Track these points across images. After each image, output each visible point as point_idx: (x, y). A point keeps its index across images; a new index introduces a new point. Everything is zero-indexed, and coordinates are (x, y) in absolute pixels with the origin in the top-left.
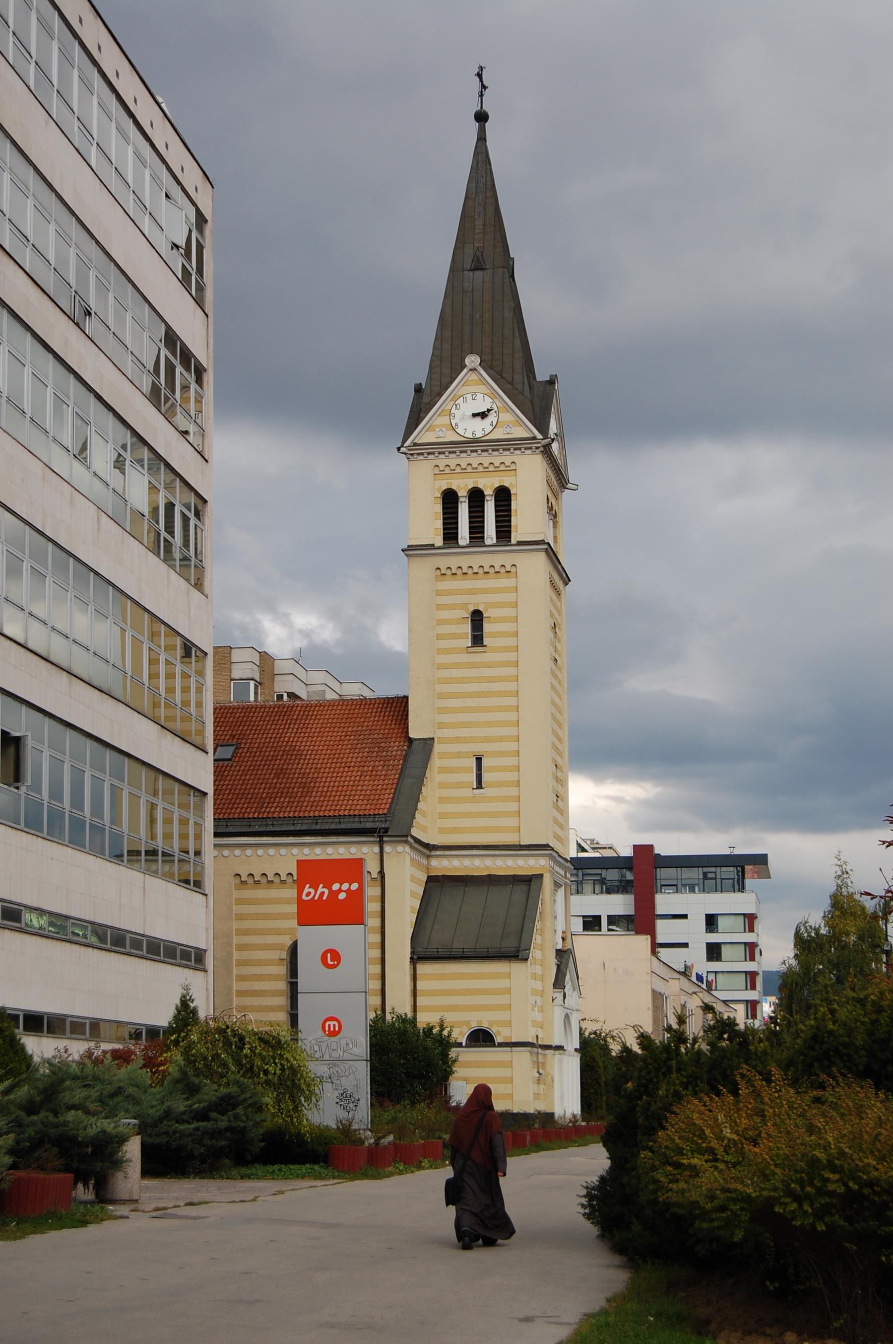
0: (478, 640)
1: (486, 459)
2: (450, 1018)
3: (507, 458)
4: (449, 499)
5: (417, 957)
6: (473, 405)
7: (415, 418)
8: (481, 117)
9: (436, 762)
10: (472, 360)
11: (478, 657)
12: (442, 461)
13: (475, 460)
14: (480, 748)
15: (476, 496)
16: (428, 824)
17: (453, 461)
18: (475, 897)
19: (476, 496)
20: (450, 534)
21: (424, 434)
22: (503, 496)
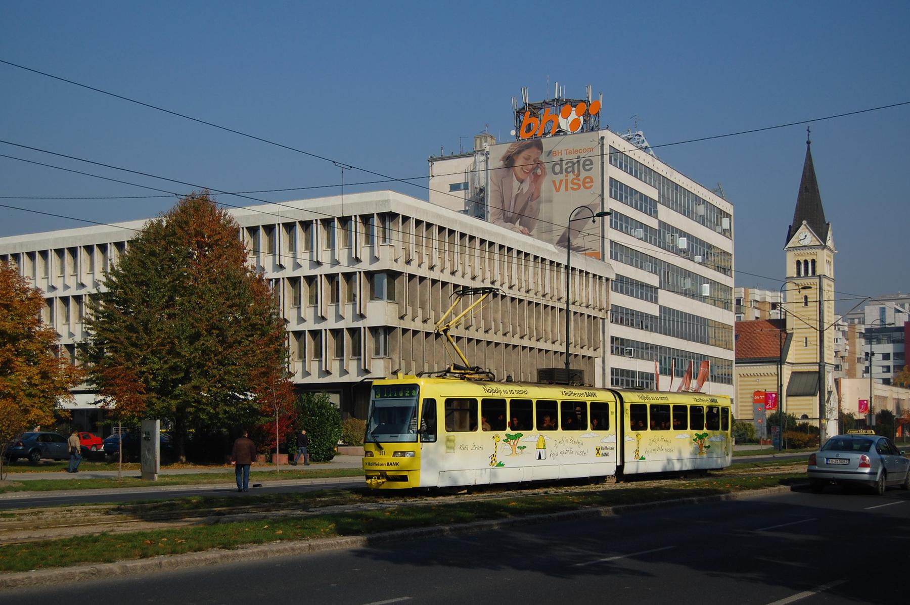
0: (806, 304)
1: (808, 251)
2: (795, 412)
3: (814, 251)
4: (799, 263)
5: (788, 395)
6: (805, 236)
7: (789, 239)
8: (808, 143)
9: (794, 338)
10: (804, 222)
11: (806, 309)
12: (796, 252)
13: (805, 252)
14: (807, 335)
15: (806, 262)
16: (790, 359)
17: (799, 252)
18: (805, 377)
19: (806, 262)
20: (799, 273)
21: (790, 245)
22: (813, 261)
